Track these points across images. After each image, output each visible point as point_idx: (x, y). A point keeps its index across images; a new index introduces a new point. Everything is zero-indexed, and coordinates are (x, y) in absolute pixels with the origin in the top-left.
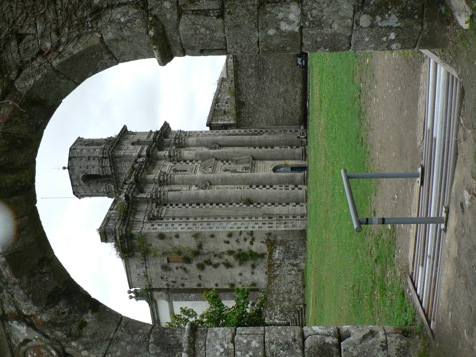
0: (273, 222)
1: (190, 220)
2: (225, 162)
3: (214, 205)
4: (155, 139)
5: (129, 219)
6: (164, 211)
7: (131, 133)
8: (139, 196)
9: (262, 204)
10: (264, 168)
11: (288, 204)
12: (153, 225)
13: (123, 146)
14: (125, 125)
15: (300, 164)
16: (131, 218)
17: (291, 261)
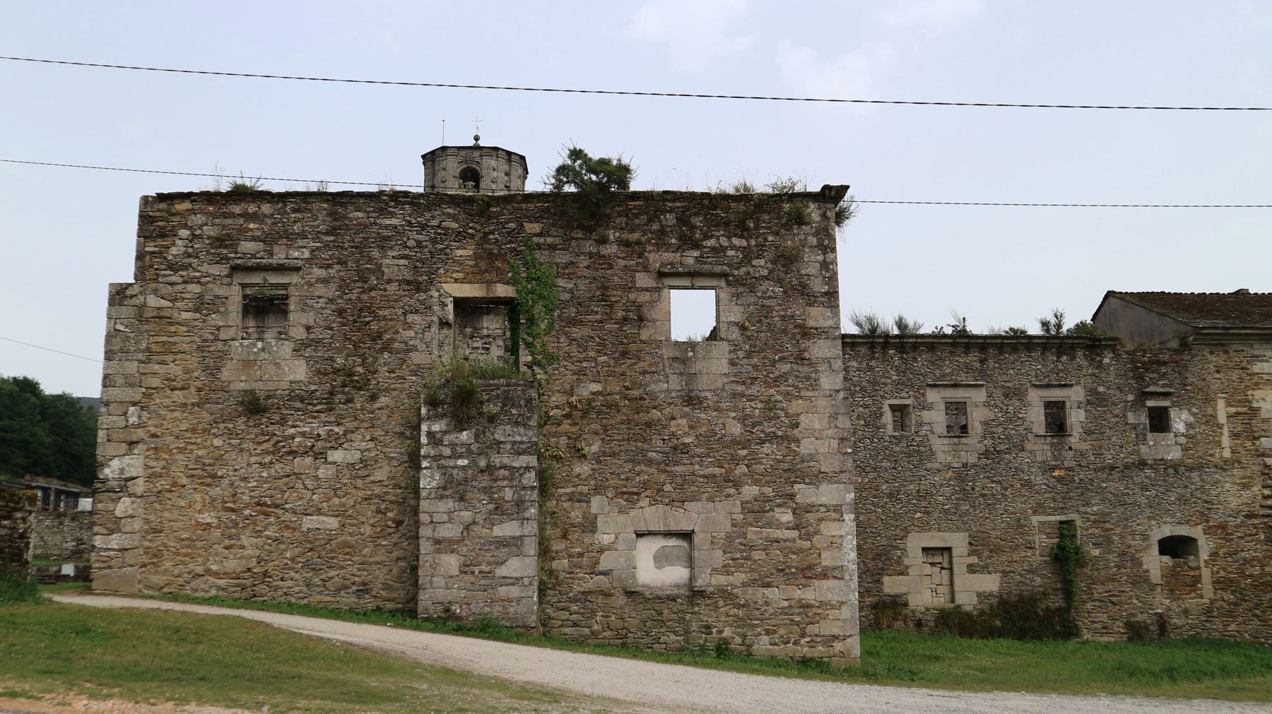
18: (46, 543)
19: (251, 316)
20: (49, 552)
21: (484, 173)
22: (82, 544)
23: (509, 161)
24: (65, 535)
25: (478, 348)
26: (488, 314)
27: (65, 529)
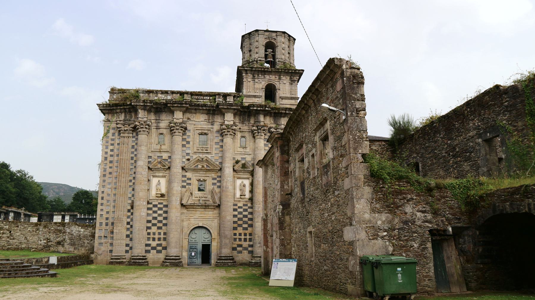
0: (108, 227)
1: (116, 158)
2: (218, 179)
4: (251, 107)
5: (117, 109)
6: (126, 135)
8: (140, 111)
9: (131, 216)
10: (203, 217)
12: (114, 129)
13: (263, 77)
14: (303, 71)
15: (212, 254)
16: (118, 111)
18: (28, 241)
19: (152, 114)
20: (30, 246)
21: (278, 44)
22: (49, 242)
23: (289, 40)
24: (40, 236)
26: (284, 117)
27: (40, 232)
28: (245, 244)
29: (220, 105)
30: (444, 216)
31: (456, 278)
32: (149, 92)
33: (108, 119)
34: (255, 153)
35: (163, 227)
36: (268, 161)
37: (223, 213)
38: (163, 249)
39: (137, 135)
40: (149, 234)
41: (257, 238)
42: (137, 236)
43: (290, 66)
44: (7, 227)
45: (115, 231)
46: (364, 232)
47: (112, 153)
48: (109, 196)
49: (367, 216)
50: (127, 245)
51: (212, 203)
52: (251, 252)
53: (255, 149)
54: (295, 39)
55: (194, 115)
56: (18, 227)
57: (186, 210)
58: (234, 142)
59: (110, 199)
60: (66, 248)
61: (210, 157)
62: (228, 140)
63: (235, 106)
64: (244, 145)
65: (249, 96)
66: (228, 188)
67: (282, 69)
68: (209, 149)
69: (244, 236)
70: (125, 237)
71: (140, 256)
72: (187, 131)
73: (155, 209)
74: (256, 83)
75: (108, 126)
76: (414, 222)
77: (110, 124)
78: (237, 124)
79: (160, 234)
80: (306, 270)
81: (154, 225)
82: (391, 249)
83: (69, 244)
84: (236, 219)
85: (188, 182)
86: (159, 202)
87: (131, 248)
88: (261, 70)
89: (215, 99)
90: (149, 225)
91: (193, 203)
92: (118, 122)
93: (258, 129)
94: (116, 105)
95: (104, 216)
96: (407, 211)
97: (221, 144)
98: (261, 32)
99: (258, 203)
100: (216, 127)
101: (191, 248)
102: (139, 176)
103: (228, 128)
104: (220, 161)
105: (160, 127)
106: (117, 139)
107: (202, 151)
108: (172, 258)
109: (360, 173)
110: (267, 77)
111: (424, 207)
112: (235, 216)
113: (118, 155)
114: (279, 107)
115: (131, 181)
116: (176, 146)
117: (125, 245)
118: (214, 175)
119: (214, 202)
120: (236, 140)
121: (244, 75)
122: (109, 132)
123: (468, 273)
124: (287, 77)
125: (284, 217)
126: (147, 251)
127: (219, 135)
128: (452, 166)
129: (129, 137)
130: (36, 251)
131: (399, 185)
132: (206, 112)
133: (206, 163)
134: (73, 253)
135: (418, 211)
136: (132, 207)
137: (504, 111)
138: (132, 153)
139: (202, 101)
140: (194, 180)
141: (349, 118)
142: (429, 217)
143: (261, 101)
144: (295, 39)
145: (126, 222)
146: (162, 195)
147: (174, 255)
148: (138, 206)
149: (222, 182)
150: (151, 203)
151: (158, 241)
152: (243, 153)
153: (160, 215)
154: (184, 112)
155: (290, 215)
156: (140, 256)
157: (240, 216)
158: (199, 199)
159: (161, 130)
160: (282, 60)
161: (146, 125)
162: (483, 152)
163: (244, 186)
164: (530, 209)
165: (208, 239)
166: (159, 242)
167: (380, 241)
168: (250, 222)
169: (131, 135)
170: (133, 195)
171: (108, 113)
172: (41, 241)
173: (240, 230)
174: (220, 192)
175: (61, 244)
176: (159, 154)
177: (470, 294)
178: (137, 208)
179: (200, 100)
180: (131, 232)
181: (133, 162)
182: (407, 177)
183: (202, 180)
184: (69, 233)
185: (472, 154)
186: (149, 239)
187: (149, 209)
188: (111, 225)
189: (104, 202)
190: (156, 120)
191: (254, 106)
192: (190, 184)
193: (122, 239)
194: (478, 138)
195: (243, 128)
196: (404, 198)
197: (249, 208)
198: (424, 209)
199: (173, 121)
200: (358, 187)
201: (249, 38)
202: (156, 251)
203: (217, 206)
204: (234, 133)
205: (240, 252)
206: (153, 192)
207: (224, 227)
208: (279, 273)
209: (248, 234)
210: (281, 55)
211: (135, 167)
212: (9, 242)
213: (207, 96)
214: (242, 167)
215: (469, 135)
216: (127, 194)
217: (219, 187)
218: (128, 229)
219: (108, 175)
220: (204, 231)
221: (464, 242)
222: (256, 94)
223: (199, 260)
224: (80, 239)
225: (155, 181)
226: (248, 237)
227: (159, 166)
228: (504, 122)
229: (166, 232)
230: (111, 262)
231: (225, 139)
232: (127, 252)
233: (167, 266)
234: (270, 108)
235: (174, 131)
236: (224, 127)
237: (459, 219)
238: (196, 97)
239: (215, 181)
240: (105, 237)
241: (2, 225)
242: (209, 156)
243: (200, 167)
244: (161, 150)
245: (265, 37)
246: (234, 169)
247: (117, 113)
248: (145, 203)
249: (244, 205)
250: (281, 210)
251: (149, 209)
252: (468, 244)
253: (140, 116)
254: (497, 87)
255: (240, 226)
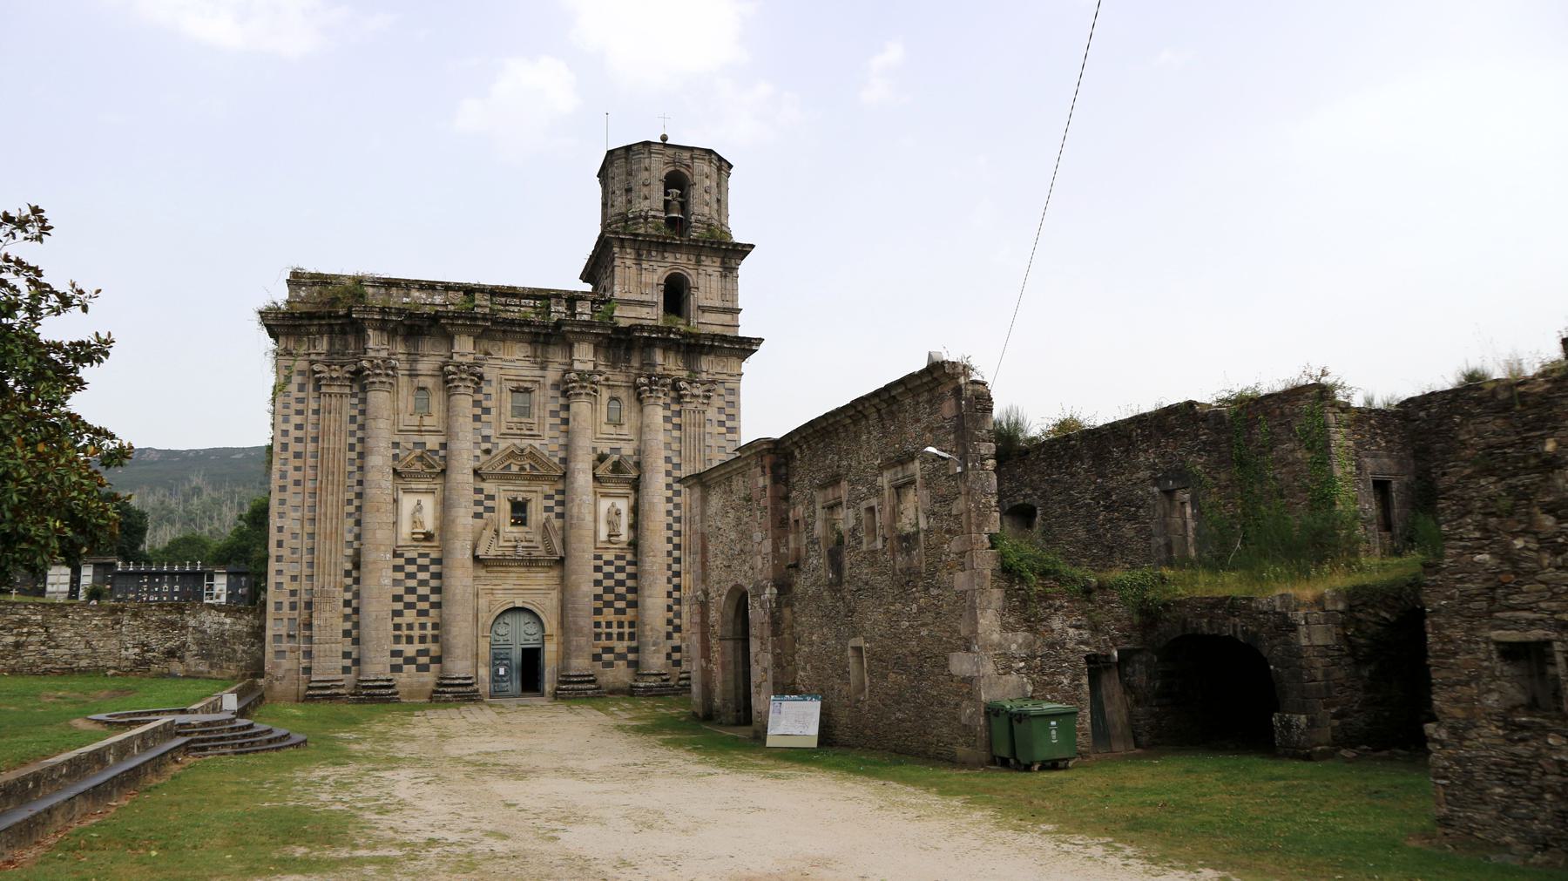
0: (297, 612)
1: (311, 447)
2: (557, 497)
3: (357, 489)
4: (635, 330)
5: (310, 325)
6: (335, 390)
7: (733, 265)
9: (355, 587)
11: (356, 641)
12: (301, 373)
14: (752, 246)
15: (547, 670)
16: (313, 329)
17: (194, 648)
18: (94, 650)
19: (399, 339)
20: (101, 663)
21: (696, 178)
22: (147, 651)
23: (719, 169)
24: (125, 638)
25: (698, 396)
26: (707, 354)
28: (621, 646)
29: (566, 325)
30: (1108, 633)
31: (1120, 729)
32: (389, 284)
33: (286, 348)
34: (644, 438)
35: (431, 611)
36: (713, 478)
37: (574, 577)
38: (432, 662)
39: (364, 389)
40: (397, 627)
41: (648, 633)
42: (373, 633)
43: (722, 232)
44: (39, 617)
45: (315, 622)
46: (992, 664)
47: (299, 434)
48: (296, 538)
49: (996, 637)
50: (346, 655)
51: (543, 553)
52: (635, 664)
53: (641, 428)
54: (730, 166)
55: (501, 344)
56: (66, 616)
57: (484, 571)
58: (594, 410)
59: (299, 546)
60: (188, 665)
61: (538, 446)
62: (581, 407)
63: (599, 327)
64: (615, 417)
65: (628, 303)
66: (584, 520)
67: (704, 242)
68: (535, 427)
69: (619, 627)
70: (341, 635)
71: (383, 680)
72: (482, 384)
73: (411, 568)
74: (643, 272)
75: (287, 367)
76: (1065, 644)
77: (291, 363)
78: (601, 368)
79: (423, 626)
80: (843, 717)
81: (410, 606)
82: (1030, 688)
83: (196, 655)
84: (599, 590)
85: (488, 503)
86: (421, 551)
87: (357, 662)
88: (657, 242)
89: (548, 307)
90: (399, 606)
91: (500, 553)
92: (313, 357)
93: (650, 382)
94: (310, 316)
95: (285, 586)
96: (1054, 627)
97: (563, 414)
98: (657, 147)
99: (651, 554)
100: (553, 374)
101: (497, 658)
102: (374, 491)
103: (583, 380)
104: (562, 454)
105: (419, 373)
106: (310, 399)
107: (519, 432)
108: (457, 682)
109: (986, 566)
110: (670, 257)
111: (1079, 620)
112: (597, 583)
113: (315, 440)
114: (695, 331)
115: (350, 502)
116: (461, 420)
117: (340, 654)
118: (547, 489)
119: (550, 552)
120: (598, 407)
121: (616, 250)
122: (290, 382)
123: (1138, 720)
124: (715, 259)
125: (780, 611)
126: (396, 668)
127: (558, 394)
128: (1103, 525)
129: (341, 396)
130: (121, 675)
131: (1043, 585)
132: (529, 338)
133: (529, 461)
134: (207, 675)
135: (1070, 627)
136: (357, 565)
137: (1200, 450)
138: (352, 434)
139: (516, 309)
140: (502, 500)
141: (970, 473)
142: (1086, 635)
143: (654, 315)
144: (730, 166)
145: (342, 601)
146: (428, 537)
147: (462, 676)
148: (375, 562)
149: (569, 506)
150: (401, 555)
151: (420, 642)
152: (614, 436)
153: (423, 583)
154: (477, 339)
155: (792, 605)
156: (383, 680)
157: (609, 583)
158: (515, 544)
159: (421, 378)
160: (704, 219)
161: (386, 369)
162: (1160, 511)
163: (618, 513)
164: (1235, 632)
165: (536, 637)
166: (422, 647)
167: (1014, 677)
168: (630, 597)
169: (347, 390)
170: (358, 537)
171: (287, 335)
172: (127, 649)
173: (609, 614)
174: (563, 528)
175: (175, 657)
176: (417, 438)
177: (1138, 755)
178: (370, 567)
179: (512, 309)
180: (357, 625)
181: (354, 455)
182: (1056, 571)
183: (520, 499)
184: (194, 628)
185: (1141, 510)
186: (397, 639)
187: (397, 568)
188: (305, 609)
189: (285, 552)
190: (409, 354)
191: (642, 328)
192: (491, 510)
193: (333, 640)
194: (1154, 485)
195: (615, 378)
196: (1051, 606)
197: (629, 563)
198: (1079, 623)
199: (451, 358)
200: (983, 590)
201: (626, 159)
202: (414, 666)
203: (557, 561)
204: (596, 391)
205: (609, 664)
206: (405, 529)
207: (576, 609)
208: (784, 722)
209: (626, 624)
210: (700, 208)
211: (361, 468)
212: (45, 654)
213: (527, 297)
214: (613, 471)
215: (1138, 475)
216: (342, 535)
217: (561, 516)
218: (346, 618)
219: (291, 488)
220: (526, 618)
221: (1133, 672)
222: (643, 298)
223: (516, 685)
224: (225, 642)
225: (408, 503)
226: (627, 630)
227: (418, 466)
228: (1199, 467)
229: (438, 621)
230: (310, 695)
231: (575, 404)
232: (346, 670)
233: (447, 701)
234: (680, 335)
235: (456, 384)
236: (573, 375)
237: (1129, 637)
238: (503, 299)
239: (551, 503)
240: (289, 636)
241: (25, 612)
242: (536, 443)
243: (515, 469)
244: (423, 429)
245: (667, 159)
246: (594, 474)
247: (308, 334)
248: (389, 556)
249: (618, 557)
250: (774, 596)
251: (397, 568)
252: (1140, 678)
253: (371, 344)
254: (1190, 404)
255: (609, 604)
